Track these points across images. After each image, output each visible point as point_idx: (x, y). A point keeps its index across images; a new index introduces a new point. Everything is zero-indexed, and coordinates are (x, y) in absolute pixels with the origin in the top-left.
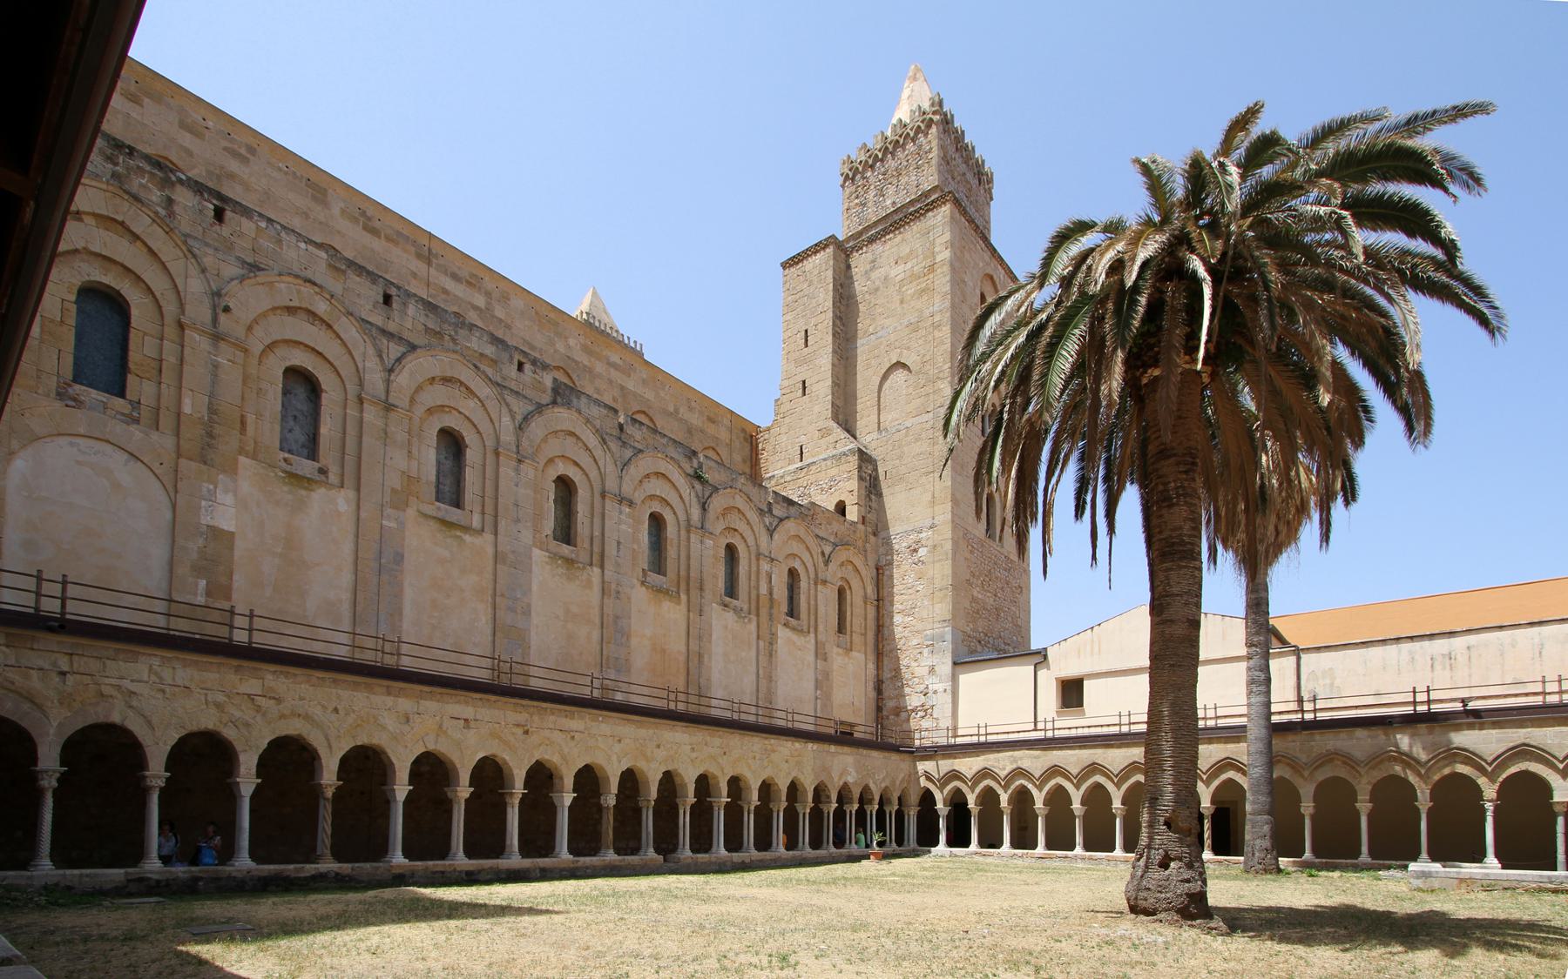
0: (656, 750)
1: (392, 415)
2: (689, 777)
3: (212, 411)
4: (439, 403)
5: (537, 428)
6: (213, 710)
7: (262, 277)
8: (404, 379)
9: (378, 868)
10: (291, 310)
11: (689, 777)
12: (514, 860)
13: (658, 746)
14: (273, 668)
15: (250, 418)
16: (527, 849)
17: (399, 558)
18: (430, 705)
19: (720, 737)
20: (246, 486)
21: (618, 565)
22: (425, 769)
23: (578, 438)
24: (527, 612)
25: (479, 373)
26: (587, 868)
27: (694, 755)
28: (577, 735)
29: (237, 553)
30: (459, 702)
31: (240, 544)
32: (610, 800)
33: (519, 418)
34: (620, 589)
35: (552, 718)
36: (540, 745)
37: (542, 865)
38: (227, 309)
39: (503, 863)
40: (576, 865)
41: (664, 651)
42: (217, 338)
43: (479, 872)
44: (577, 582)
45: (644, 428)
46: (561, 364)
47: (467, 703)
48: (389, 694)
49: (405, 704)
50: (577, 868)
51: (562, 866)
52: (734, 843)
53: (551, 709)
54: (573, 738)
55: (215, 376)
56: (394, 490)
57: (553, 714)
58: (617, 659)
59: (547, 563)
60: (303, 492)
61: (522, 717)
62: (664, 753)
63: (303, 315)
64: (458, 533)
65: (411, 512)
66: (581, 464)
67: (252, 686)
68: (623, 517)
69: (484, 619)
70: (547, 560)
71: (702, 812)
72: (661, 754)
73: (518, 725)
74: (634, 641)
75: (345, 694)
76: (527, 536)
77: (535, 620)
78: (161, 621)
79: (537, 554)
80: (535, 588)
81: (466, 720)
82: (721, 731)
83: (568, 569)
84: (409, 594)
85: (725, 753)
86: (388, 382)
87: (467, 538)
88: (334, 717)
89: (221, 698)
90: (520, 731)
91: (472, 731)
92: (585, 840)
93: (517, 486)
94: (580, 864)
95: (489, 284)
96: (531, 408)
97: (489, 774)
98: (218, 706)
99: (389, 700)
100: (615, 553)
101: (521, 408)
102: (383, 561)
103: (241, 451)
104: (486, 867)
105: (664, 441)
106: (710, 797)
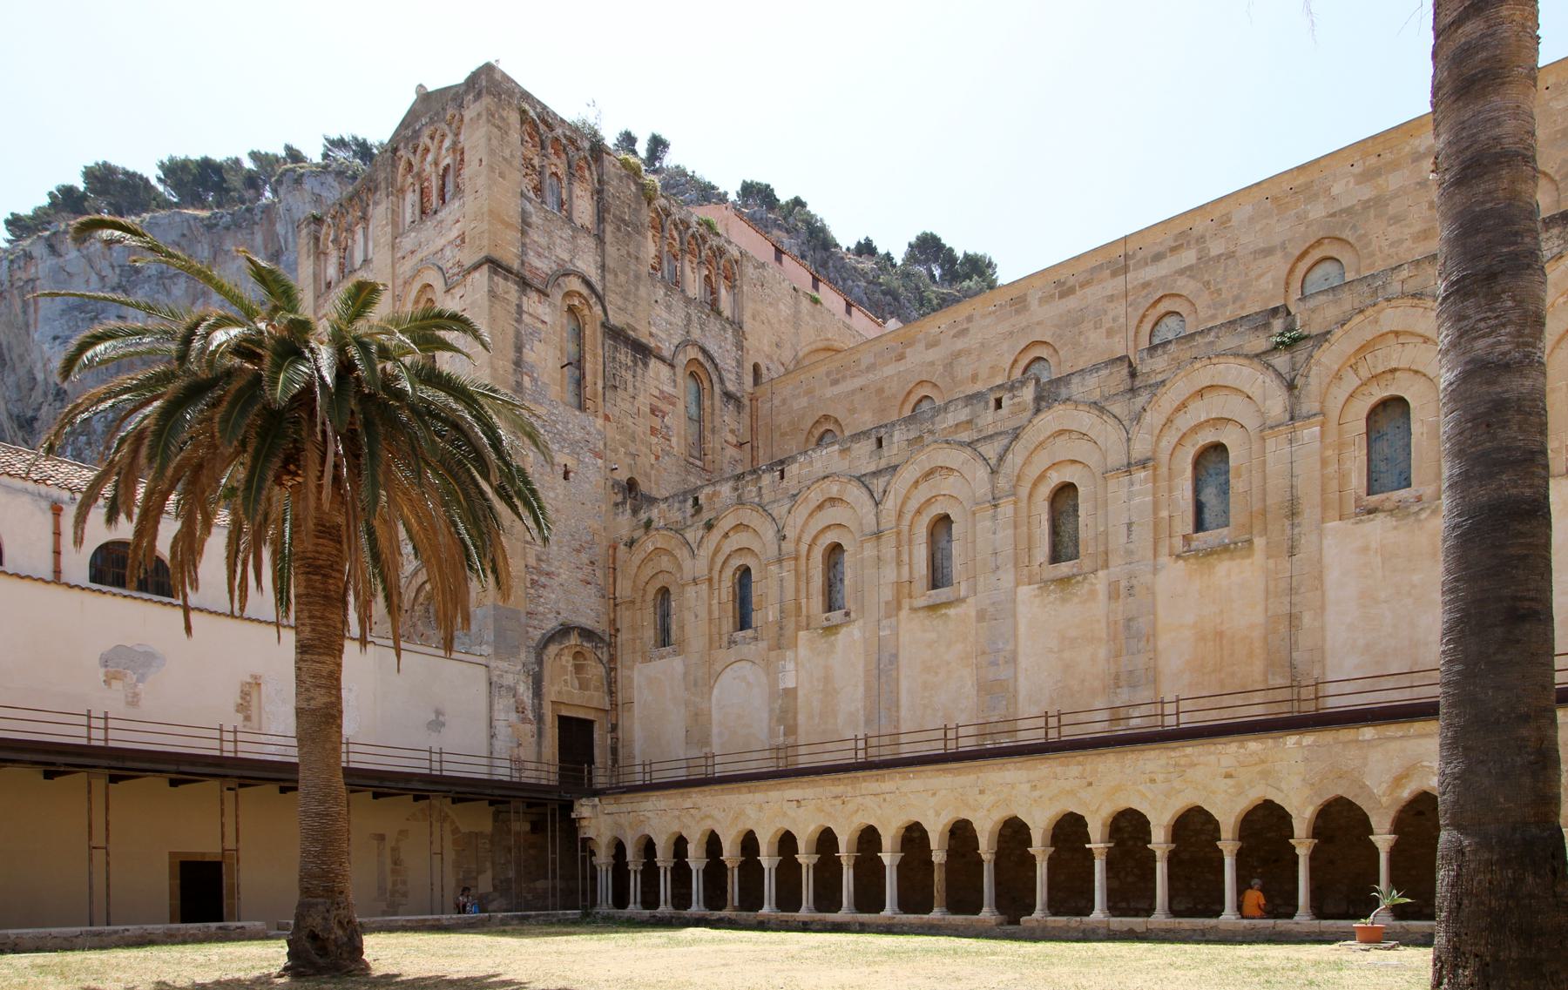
0: (979, 797)
1: (883, 539)
2: (805, 837)
3: (782, 612)
4: (923, 500)
5: (1015, 459)
6: (677, 821)
7: (800, 499)
8: (890, 504)
9: (748, 916)
10: (820, 507)
11: (805, 837)
12: (843, 915)
13: (982, 792)
14: (696, 789)
15: (804, 601)
16: (905, 905)
17: (895, 657)
18: (774, 795)
19: (1079, 764)
20: (803, 651)
21: (1130, 553)
22: (1123, 824)
23: (1070, 431)
24: (1013, 659)
25: (954, 446)
26: (903, 925)
27: (1037, 794)
28: (887, 796)
29: (799, 700)
30: (791, 788)
31: (800, 693)
32: (938, 857)
33: (993, 462)
34: (1134, 582)
35: (864, 784)
36: (857, 811)
37: (861, 920)
38: (784, 537)
39: (725, 913)
40: (891, 922)
41: (1220, 635)
42: (780, 561)
43: (812, 922)
44: (1076, 600)
45: (1172, 348)
46: (1321, 234)
47: (797, 787)
48: (750, 792)
49: (759, 797)
50: (893, 925)
51: (880, 922)
52: (650, 900)
53: (863, 777)
54: (885, 800)
55: (781, 586)
56: (887, 603)
57: (865, 781)
58: (1131, 672)
59: (1035, 596)
60: (833, 638)
61: (839, 789)
62: (992, 798)
63: (827, 504)
64: (943, 611)
65: (904, 613)
66: (87, 823)
67: (688, 803)
68: (1136, 487)
69: (970, 683)
70: (1036, 592)
71: (681, 871)
72: (988, 799)
73: (836, 797)
74: (1163, 641)
75: (726, 797)
76: (1007, 578)
77: (1023, 662)
78: (683, 772)
79: (1025, 591)
80: (1022, 629)
81: (798, 801)
82: (1079, 756)
83: (1062, 590)
84: (904, 685)
85: (1090, 784)
86: (877, 515)
87: (952, 612)
88: (723, 814)
89: (677, 813)
90: (838, 802)
91: (802, 809)
92: (915, 899)
93: (994, 533)
94: (895, 921)
95: (1200, 226)
96: (1006, 441)
97: (1014, 833)
98: (679, 817)
99: (750, 797)
100: (1123, 539)
101: (991, 450)
102: (881, 666)
103: (798, 628)
104: (816, 919)
105: (1211, 337)
106: (1090, 843)
